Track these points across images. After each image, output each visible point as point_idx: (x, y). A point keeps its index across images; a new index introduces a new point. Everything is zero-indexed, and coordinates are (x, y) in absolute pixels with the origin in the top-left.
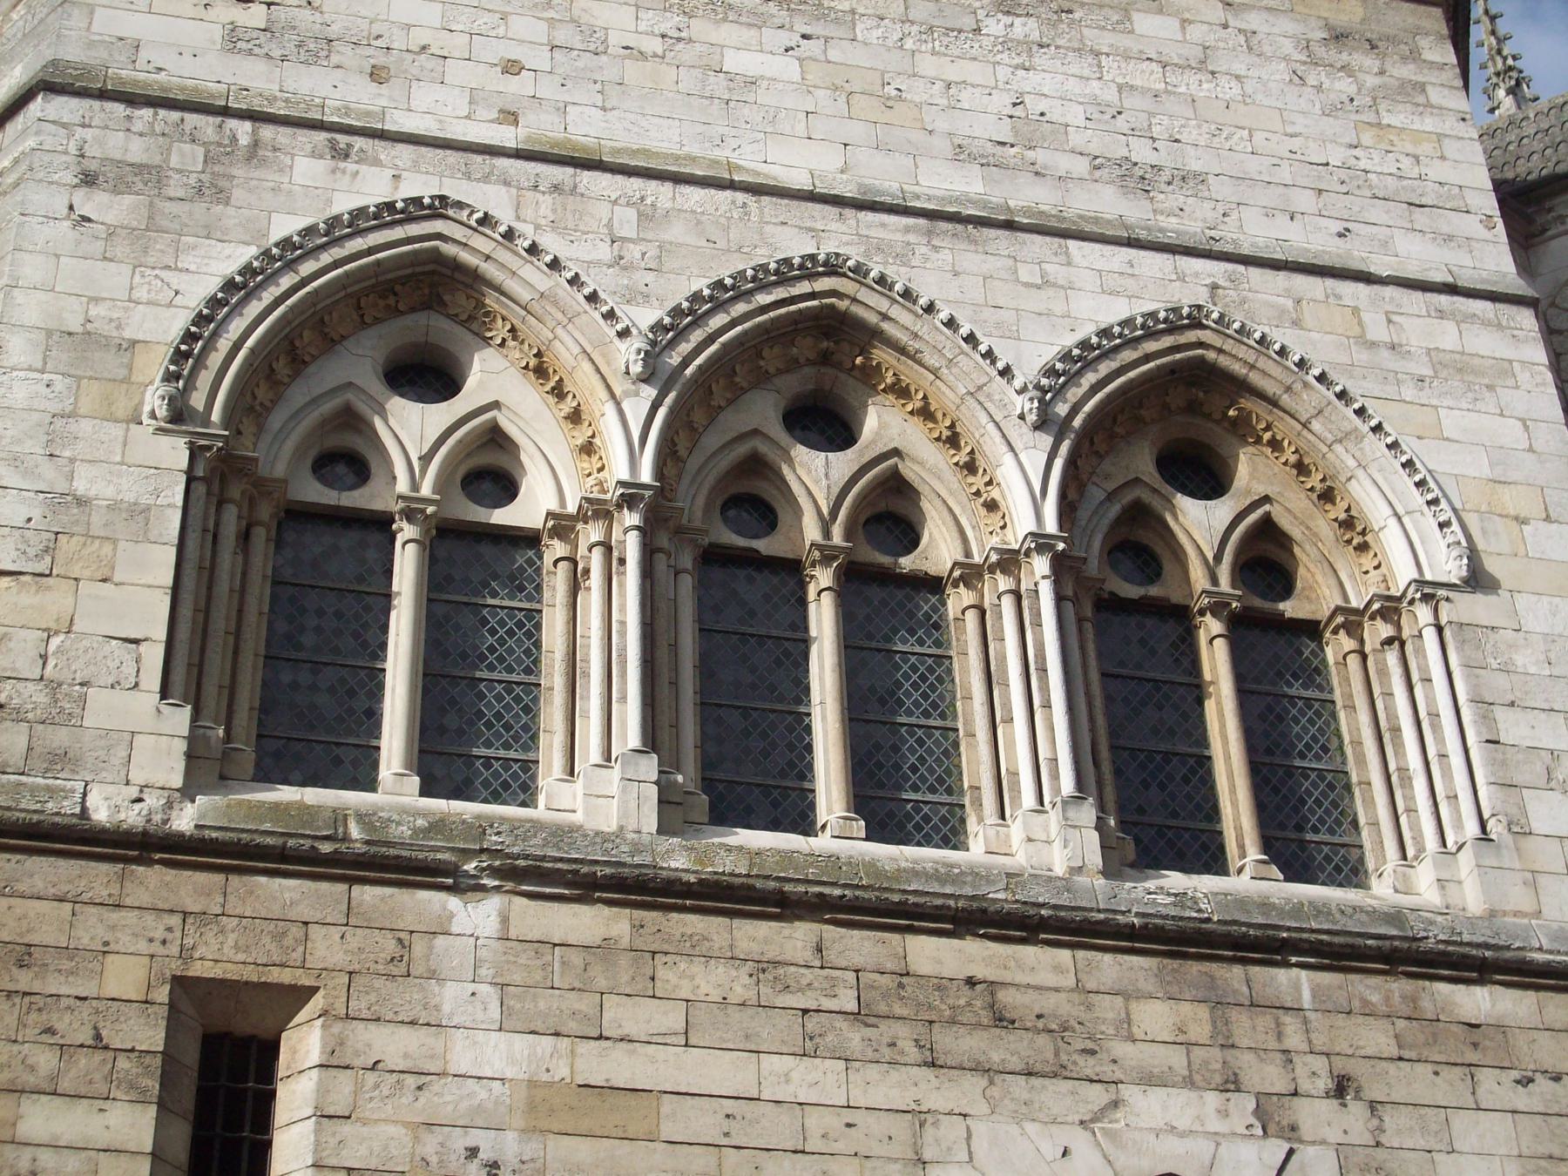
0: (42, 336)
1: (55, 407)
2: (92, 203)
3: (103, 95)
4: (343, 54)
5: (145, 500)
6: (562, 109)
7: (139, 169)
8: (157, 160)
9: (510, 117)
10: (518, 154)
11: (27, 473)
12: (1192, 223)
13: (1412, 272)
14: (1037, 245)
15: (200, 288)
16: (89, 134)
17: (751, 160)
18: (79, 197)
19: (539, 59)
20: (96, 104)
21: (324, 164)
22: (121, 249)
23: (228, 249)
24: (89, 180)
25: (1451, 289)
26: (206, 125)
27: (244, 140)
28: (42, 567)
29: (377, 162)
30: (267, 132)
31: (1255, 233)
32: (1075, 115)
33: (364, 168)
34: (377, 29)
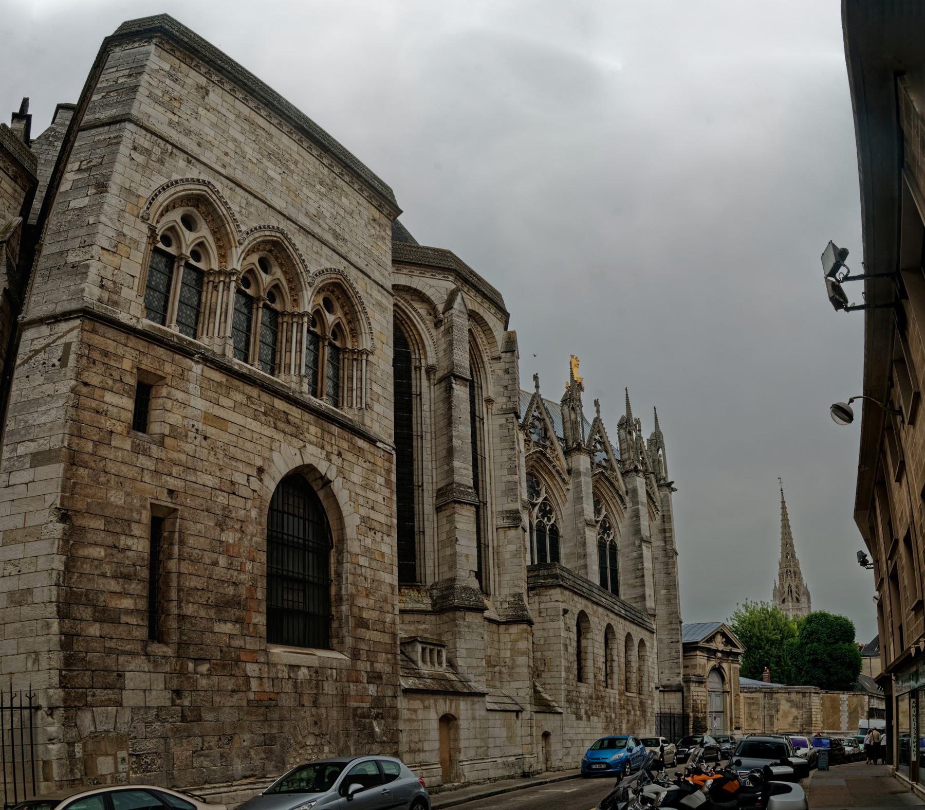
0: (119, 187)
1: (121, 208)
2: (135, 155)
3: (142, 127)
4: (193, 136)
5: (138, 239)
6: (235, 169)
7: (147, 149)
8: (150, 149)
9: (224, 166)
10: (226, 177)
11: (113, 223)
12: (343, 250)
13: (376, 279)
14: (317, 243)
15: (155, 186)
16: (137, 136)
17: (269, 197)
18: (132, 152)
19: (232, 154)
20: (139, 128)
21: (186, 163)
22: (140, 170)
23: (163, 178)
24: (135, 149)
25: (382, 287)
26: (162, 143)
27: (170, 151)
28: (114, 250)
29: (196, 167)
30: (175, 150)
31: (353, 258)
32: (328, 215)
33: (194, 168)
34: (201, 132)
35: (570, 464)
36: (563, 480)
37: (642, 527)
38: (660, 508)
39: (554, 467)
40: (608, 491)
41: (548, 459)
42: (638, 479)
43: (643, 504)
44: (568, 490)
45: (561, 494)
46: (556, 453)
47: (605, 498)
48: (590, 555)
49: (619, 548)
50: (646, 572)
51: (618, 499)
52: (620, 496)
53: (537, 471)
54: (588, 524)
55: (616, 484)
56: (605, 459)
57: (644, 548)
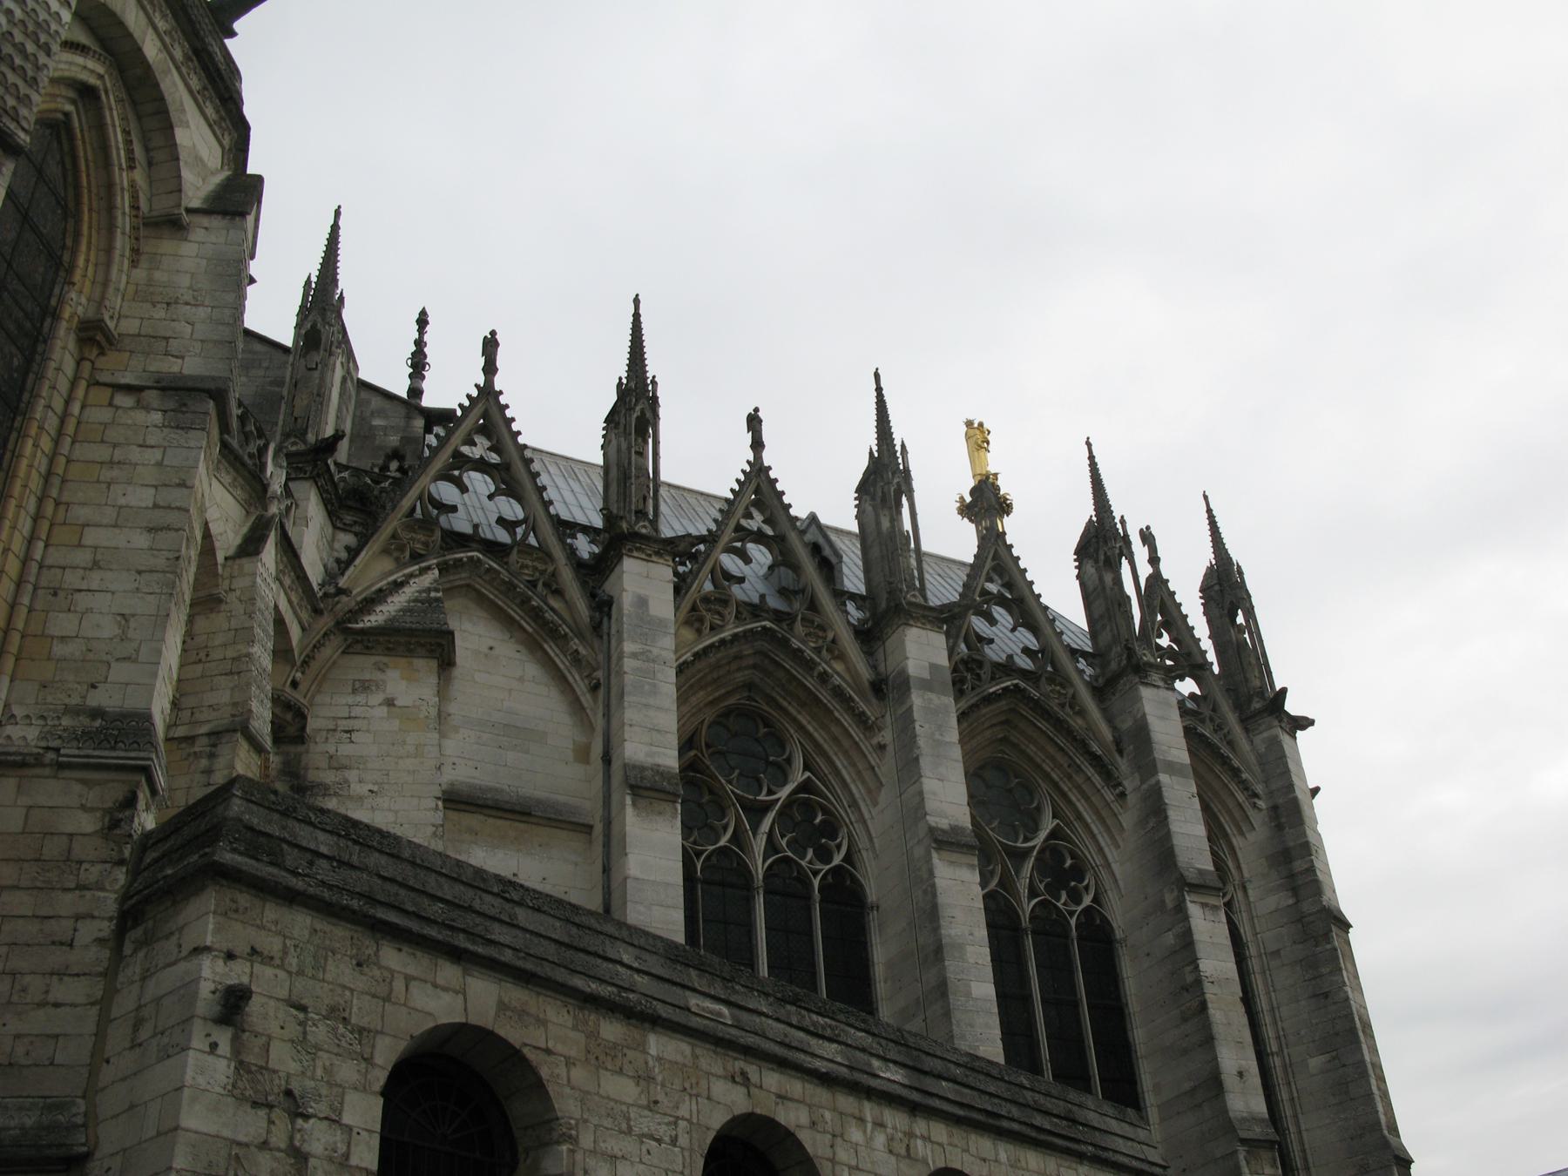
35: (882, 668)
36: (861, 719)
37: (1179, 842)
38: (1259, 789)
39: (824, 678)
40: (1051, 750)
41: (797, 655)
42: (1146, 692)
43: (1172, 768)
44: (882, 747)
45: (861, 766)
46: (830, 636)
47: (1047, 776)
48: (960, 947)
49: (1119, 934)
50: (1210, 992)
51: (1090, 771)
52: (1096, 760)
53: (771, 701)
54: (946, 841)
55: (1077, 723)
56: (1026, 651)
57: (1194, 910)
